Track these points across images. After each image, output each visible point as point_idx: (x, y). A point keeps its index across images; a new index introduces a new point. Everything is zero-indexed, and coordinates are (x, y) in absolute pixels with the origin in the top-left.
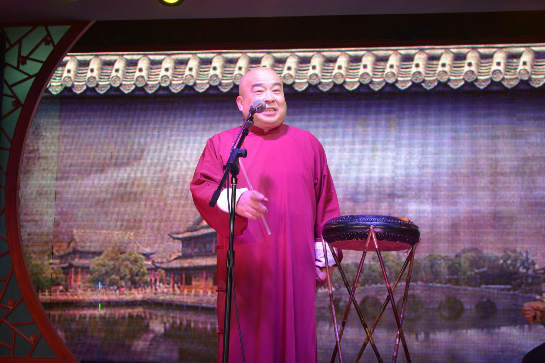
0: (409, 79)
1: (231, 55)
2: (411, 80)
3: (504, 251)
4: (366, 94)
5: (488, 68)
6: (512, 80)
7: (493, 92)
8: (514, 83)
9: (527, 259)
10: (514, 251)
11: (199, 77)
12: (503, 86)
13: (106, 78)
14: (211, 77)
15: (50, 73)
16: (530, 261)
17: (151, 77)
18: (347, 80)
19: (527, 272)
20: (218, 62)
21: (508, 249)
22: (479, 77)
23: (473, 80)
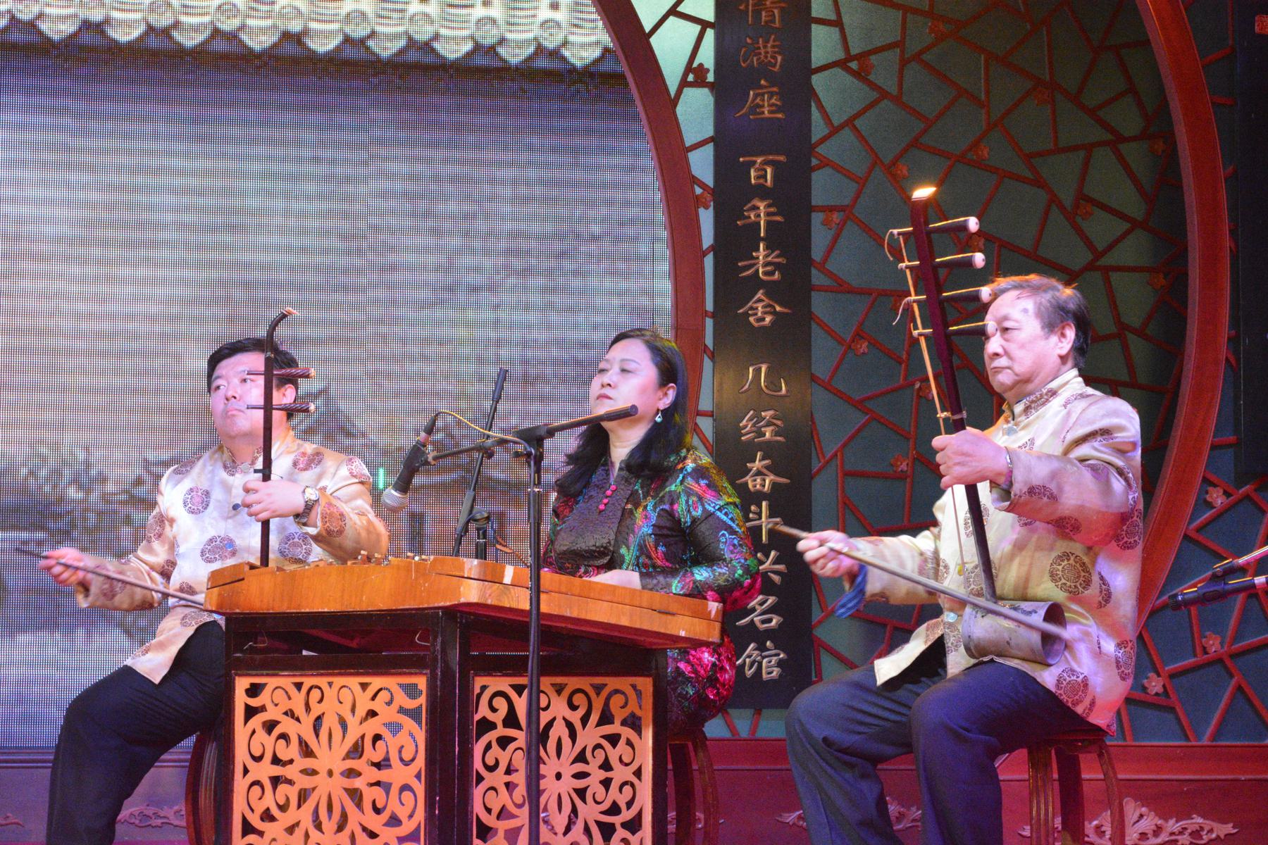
0: (466, 33)
2: (472, 38)
3: (31, 445)
4: (295, 61)
5: (531, 13)
6: (64, 18)
7: (347, 63)
8: (69, 28)
9: (88, 465)
10: (56, 446)
11: (445, 19)
12: (564, 59)
13: (395, 15)
14: (348, 15)
15: (604, 11)
16: (93, 472)
18: (314, 25)
19: (85, 500)
21: (41, 442)
22: (379, 29)
23: (494, 40)
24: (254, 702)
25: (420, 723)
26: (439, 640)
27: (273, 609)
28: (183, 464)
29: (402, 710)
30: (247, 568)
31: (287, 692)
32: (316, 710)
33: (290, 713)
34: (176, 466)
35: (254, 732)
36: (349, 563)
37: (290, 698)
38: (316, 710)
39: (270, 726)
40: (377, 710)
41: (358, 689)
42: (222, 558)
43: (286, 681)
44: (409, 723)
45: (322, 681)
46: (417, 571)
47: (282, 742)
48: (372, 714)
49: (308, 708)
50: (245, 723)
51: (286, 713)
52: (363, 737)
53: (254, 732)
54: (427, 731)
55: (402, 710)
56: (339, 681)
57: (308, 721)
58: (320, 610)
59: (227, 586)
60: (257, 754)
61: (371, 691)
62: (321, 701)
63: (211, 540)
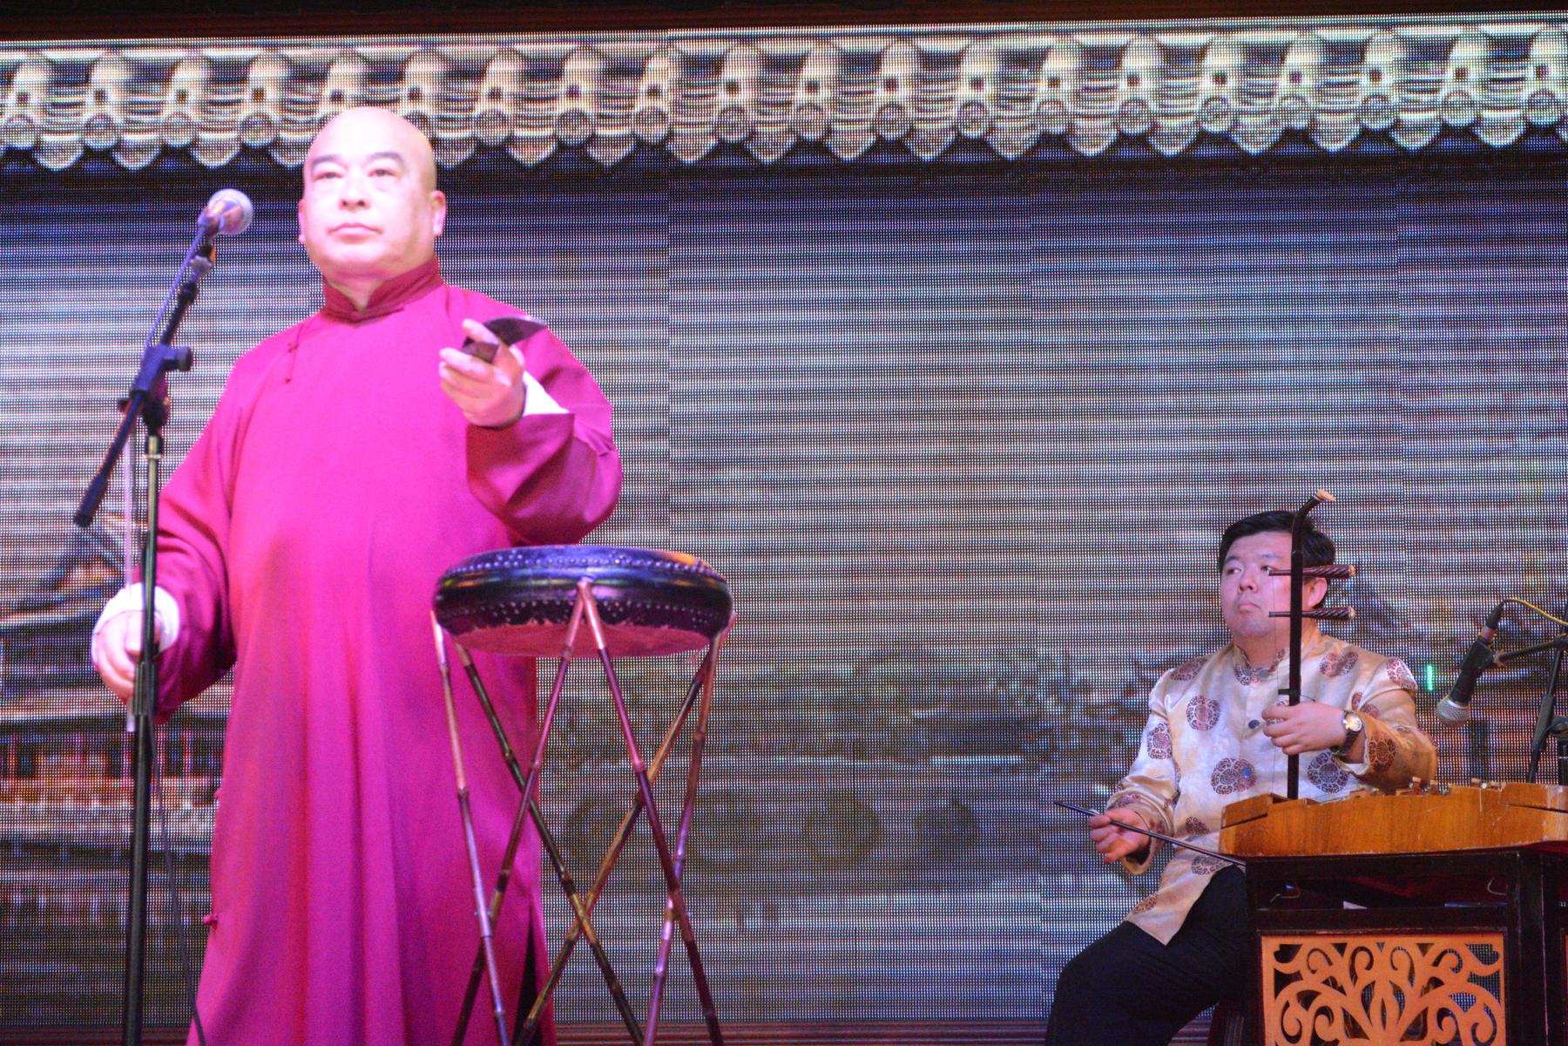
1: (306, 51)
17: (290, 116)
20: (581, 69)
24: (1286, 968)
25: (1497, 996)
26: (1518, 888)
27: (1304, 852)
28: (1183, 668)
29: (1473, 978)
30: (1270, 801)
31: (1326, 956)
32: (1365, 978)
33: (1332, 982)
34: (1172, 670)
35: (1287, 1005)
36: (1398, 792)
37: (1330, 963)
38: (1365, 978)
39: (1307, 998)
40: (1442, 978)
41: (1416, 952)
42: (1239, 787)
43: (1325, 943)
44: (1483, 995)
45: (1370, 942)
46: (1484, 803)
47: (1322, 1018)
48: (1436, 982)
49: (1354, 976)
50: (1277, 993)
51: (1326, 982)
52: (1425, 1012)
53: (1287, 1005)
54: (1506, 1006)
55: (1473, 978)
56: (1392, 942)
57: (1354, 992)
58: (1364, 853)
59: (1245, 824)
60: (1292, 1032)
61: (1433, 953)
62: (1369, 967)
63: (1222, 764)
